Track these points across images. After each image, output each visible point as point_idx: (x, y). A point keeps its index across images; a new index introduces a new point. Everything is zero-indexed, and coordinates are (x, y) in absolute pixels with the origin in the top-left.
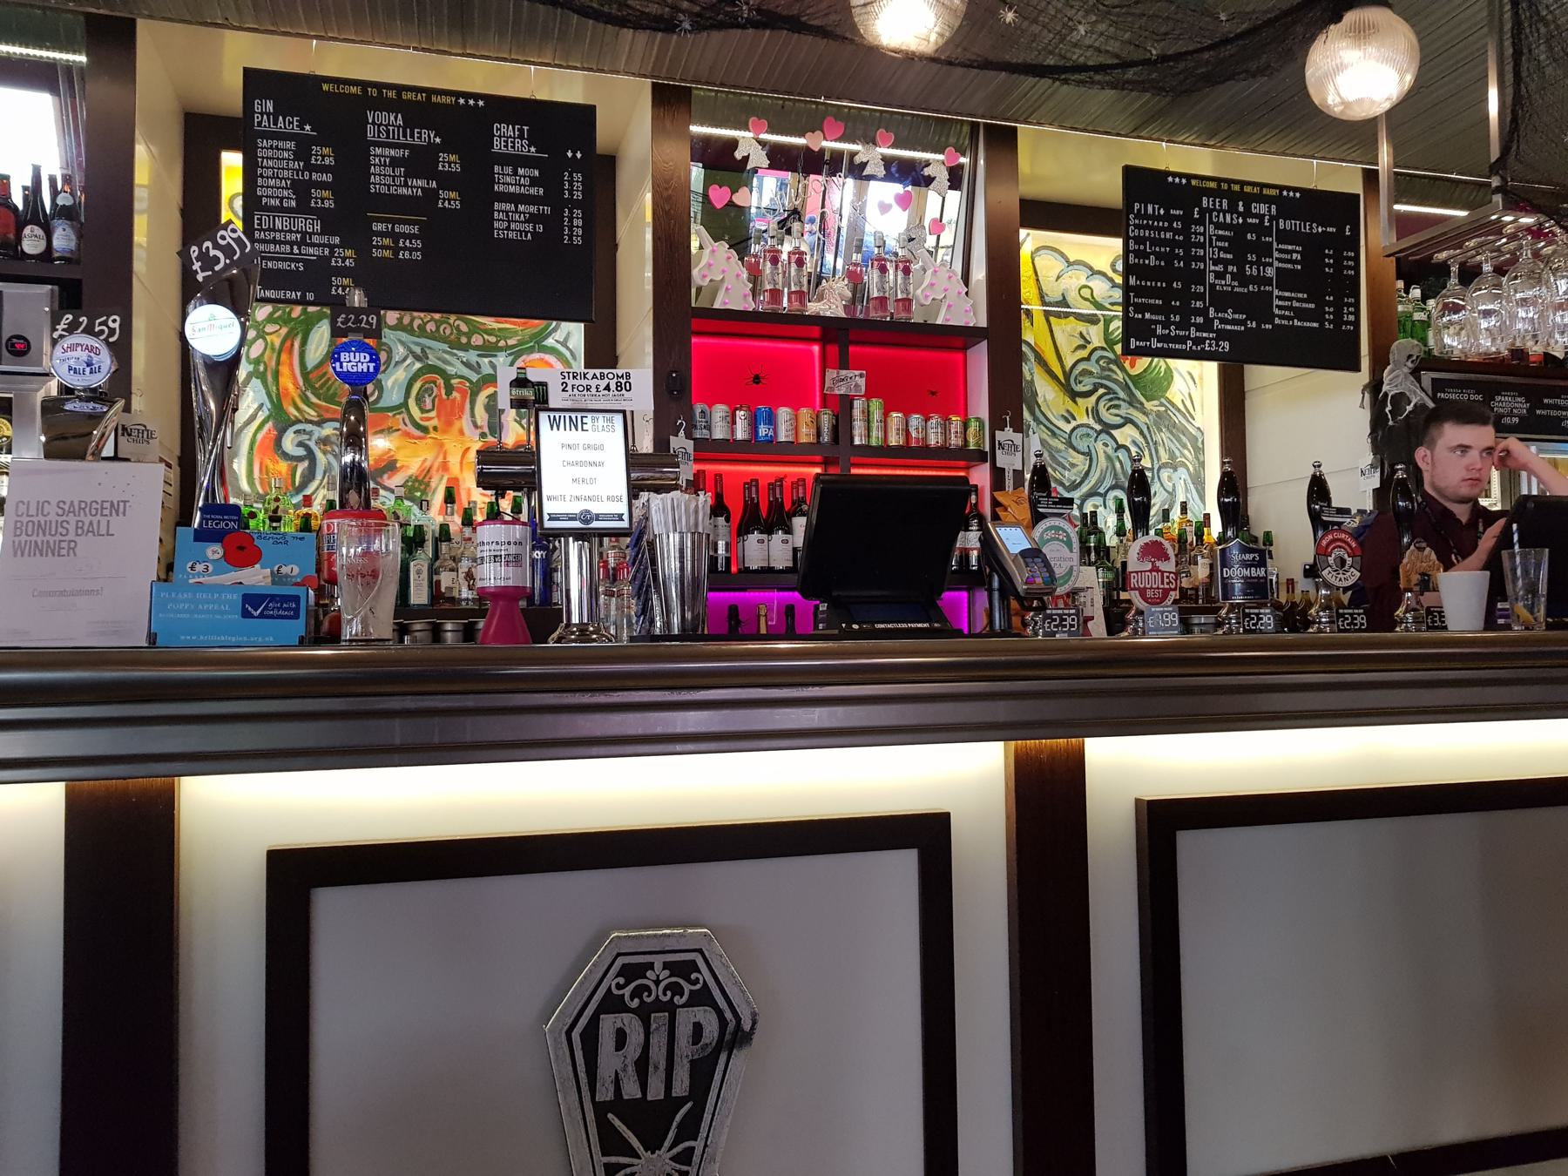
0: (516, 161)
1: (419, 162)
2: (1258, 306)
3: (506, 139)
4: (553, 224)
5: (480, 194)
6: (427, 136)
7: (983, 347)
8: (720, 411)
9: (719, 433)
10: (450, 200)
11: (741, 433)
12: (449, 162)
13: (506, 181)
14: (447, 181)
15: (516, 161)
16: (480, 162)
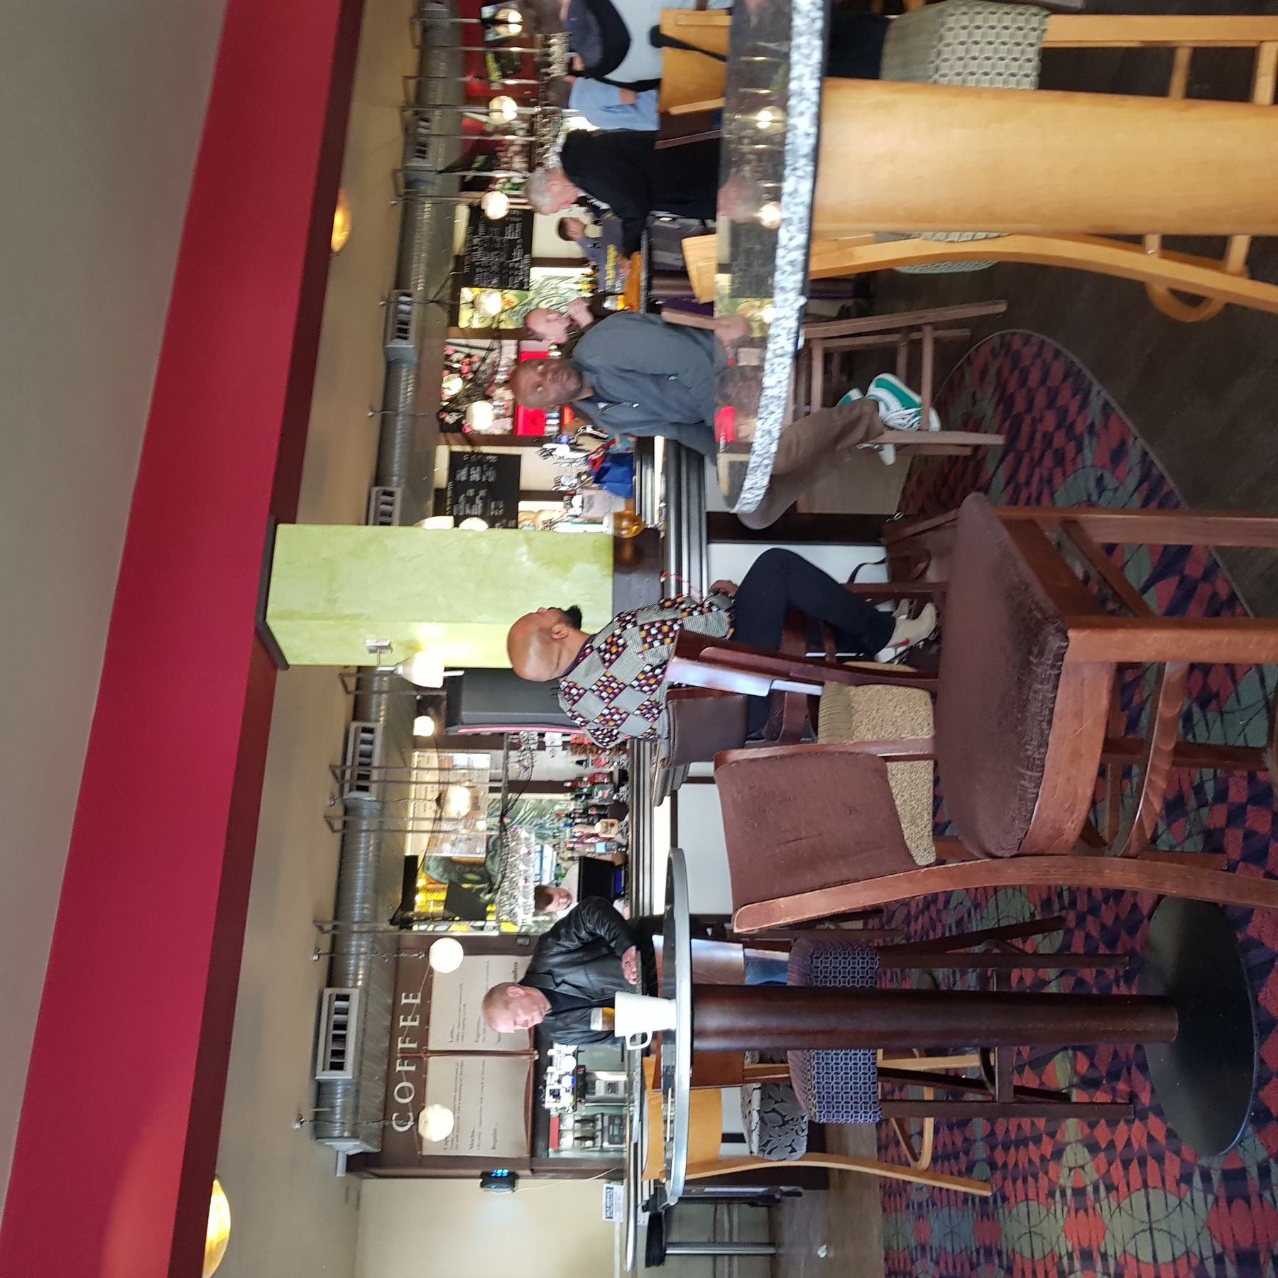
0: (469, 475)
1: (471, 501)
2: (512, 243)
3: (462, 475)
4: (490, 464)
5: (477, 486)
6: (462, 498)
7: (524, 343)
8: (548, 429)
9: (556, 429)
10: (482, 493)
11: (557, 421)
12: (471, 492)
13: (475, 476)
14: (476, 494)
15: (469, 475)
16: (469, 484)
